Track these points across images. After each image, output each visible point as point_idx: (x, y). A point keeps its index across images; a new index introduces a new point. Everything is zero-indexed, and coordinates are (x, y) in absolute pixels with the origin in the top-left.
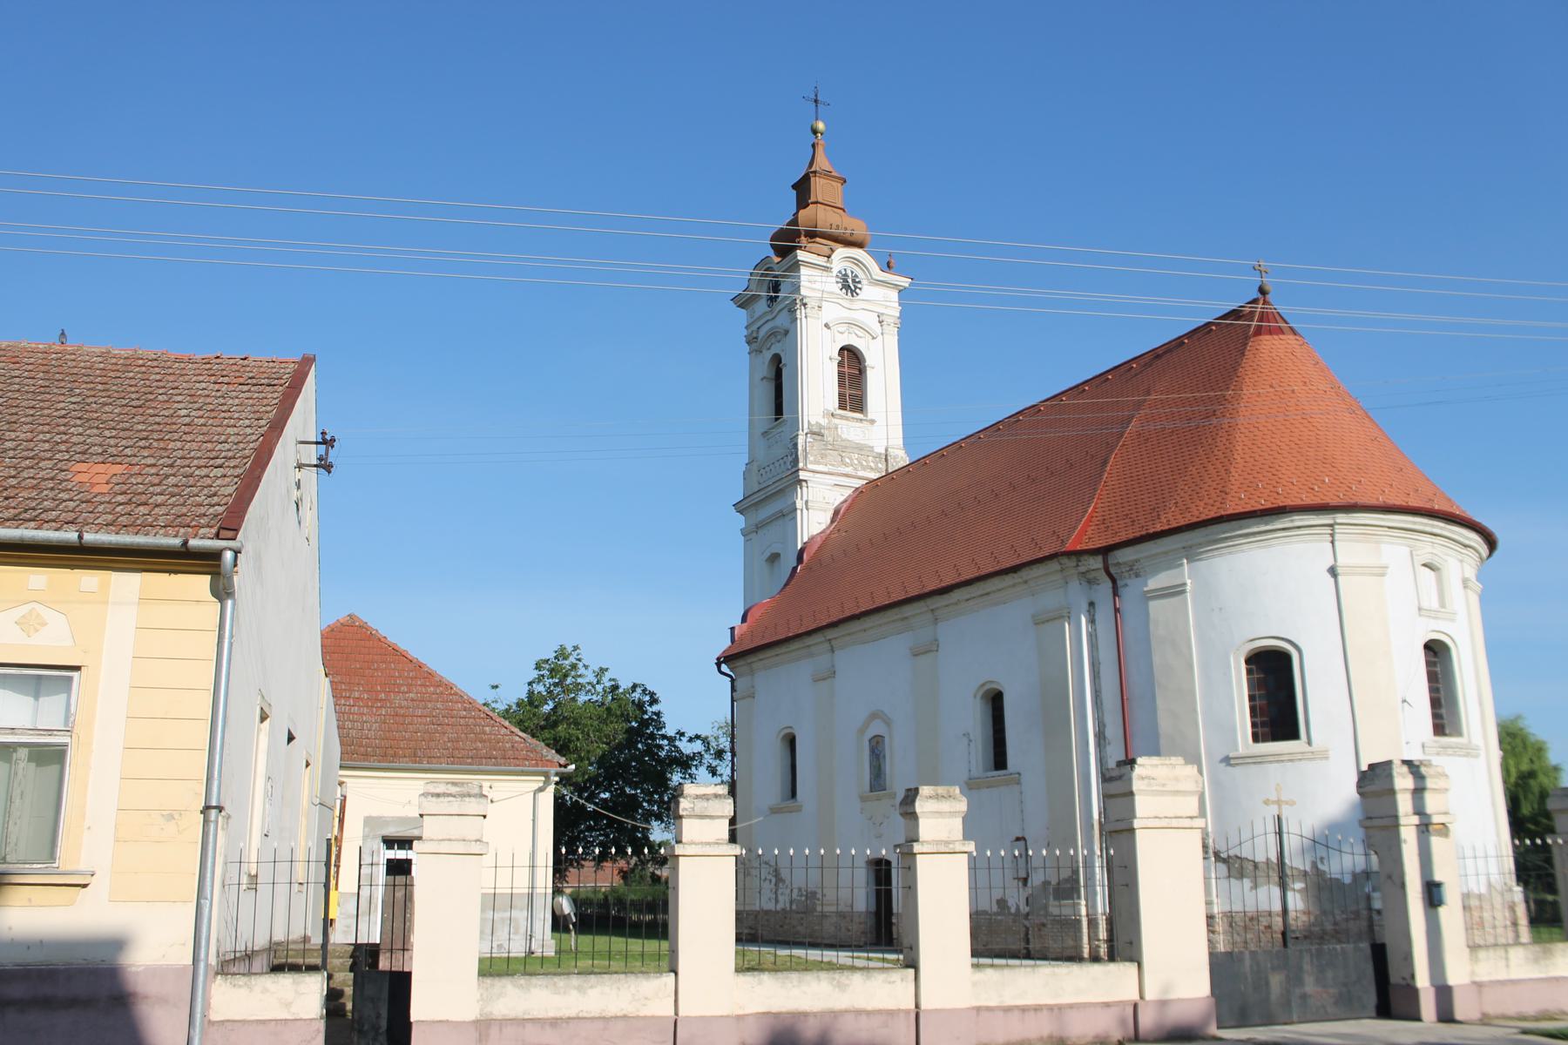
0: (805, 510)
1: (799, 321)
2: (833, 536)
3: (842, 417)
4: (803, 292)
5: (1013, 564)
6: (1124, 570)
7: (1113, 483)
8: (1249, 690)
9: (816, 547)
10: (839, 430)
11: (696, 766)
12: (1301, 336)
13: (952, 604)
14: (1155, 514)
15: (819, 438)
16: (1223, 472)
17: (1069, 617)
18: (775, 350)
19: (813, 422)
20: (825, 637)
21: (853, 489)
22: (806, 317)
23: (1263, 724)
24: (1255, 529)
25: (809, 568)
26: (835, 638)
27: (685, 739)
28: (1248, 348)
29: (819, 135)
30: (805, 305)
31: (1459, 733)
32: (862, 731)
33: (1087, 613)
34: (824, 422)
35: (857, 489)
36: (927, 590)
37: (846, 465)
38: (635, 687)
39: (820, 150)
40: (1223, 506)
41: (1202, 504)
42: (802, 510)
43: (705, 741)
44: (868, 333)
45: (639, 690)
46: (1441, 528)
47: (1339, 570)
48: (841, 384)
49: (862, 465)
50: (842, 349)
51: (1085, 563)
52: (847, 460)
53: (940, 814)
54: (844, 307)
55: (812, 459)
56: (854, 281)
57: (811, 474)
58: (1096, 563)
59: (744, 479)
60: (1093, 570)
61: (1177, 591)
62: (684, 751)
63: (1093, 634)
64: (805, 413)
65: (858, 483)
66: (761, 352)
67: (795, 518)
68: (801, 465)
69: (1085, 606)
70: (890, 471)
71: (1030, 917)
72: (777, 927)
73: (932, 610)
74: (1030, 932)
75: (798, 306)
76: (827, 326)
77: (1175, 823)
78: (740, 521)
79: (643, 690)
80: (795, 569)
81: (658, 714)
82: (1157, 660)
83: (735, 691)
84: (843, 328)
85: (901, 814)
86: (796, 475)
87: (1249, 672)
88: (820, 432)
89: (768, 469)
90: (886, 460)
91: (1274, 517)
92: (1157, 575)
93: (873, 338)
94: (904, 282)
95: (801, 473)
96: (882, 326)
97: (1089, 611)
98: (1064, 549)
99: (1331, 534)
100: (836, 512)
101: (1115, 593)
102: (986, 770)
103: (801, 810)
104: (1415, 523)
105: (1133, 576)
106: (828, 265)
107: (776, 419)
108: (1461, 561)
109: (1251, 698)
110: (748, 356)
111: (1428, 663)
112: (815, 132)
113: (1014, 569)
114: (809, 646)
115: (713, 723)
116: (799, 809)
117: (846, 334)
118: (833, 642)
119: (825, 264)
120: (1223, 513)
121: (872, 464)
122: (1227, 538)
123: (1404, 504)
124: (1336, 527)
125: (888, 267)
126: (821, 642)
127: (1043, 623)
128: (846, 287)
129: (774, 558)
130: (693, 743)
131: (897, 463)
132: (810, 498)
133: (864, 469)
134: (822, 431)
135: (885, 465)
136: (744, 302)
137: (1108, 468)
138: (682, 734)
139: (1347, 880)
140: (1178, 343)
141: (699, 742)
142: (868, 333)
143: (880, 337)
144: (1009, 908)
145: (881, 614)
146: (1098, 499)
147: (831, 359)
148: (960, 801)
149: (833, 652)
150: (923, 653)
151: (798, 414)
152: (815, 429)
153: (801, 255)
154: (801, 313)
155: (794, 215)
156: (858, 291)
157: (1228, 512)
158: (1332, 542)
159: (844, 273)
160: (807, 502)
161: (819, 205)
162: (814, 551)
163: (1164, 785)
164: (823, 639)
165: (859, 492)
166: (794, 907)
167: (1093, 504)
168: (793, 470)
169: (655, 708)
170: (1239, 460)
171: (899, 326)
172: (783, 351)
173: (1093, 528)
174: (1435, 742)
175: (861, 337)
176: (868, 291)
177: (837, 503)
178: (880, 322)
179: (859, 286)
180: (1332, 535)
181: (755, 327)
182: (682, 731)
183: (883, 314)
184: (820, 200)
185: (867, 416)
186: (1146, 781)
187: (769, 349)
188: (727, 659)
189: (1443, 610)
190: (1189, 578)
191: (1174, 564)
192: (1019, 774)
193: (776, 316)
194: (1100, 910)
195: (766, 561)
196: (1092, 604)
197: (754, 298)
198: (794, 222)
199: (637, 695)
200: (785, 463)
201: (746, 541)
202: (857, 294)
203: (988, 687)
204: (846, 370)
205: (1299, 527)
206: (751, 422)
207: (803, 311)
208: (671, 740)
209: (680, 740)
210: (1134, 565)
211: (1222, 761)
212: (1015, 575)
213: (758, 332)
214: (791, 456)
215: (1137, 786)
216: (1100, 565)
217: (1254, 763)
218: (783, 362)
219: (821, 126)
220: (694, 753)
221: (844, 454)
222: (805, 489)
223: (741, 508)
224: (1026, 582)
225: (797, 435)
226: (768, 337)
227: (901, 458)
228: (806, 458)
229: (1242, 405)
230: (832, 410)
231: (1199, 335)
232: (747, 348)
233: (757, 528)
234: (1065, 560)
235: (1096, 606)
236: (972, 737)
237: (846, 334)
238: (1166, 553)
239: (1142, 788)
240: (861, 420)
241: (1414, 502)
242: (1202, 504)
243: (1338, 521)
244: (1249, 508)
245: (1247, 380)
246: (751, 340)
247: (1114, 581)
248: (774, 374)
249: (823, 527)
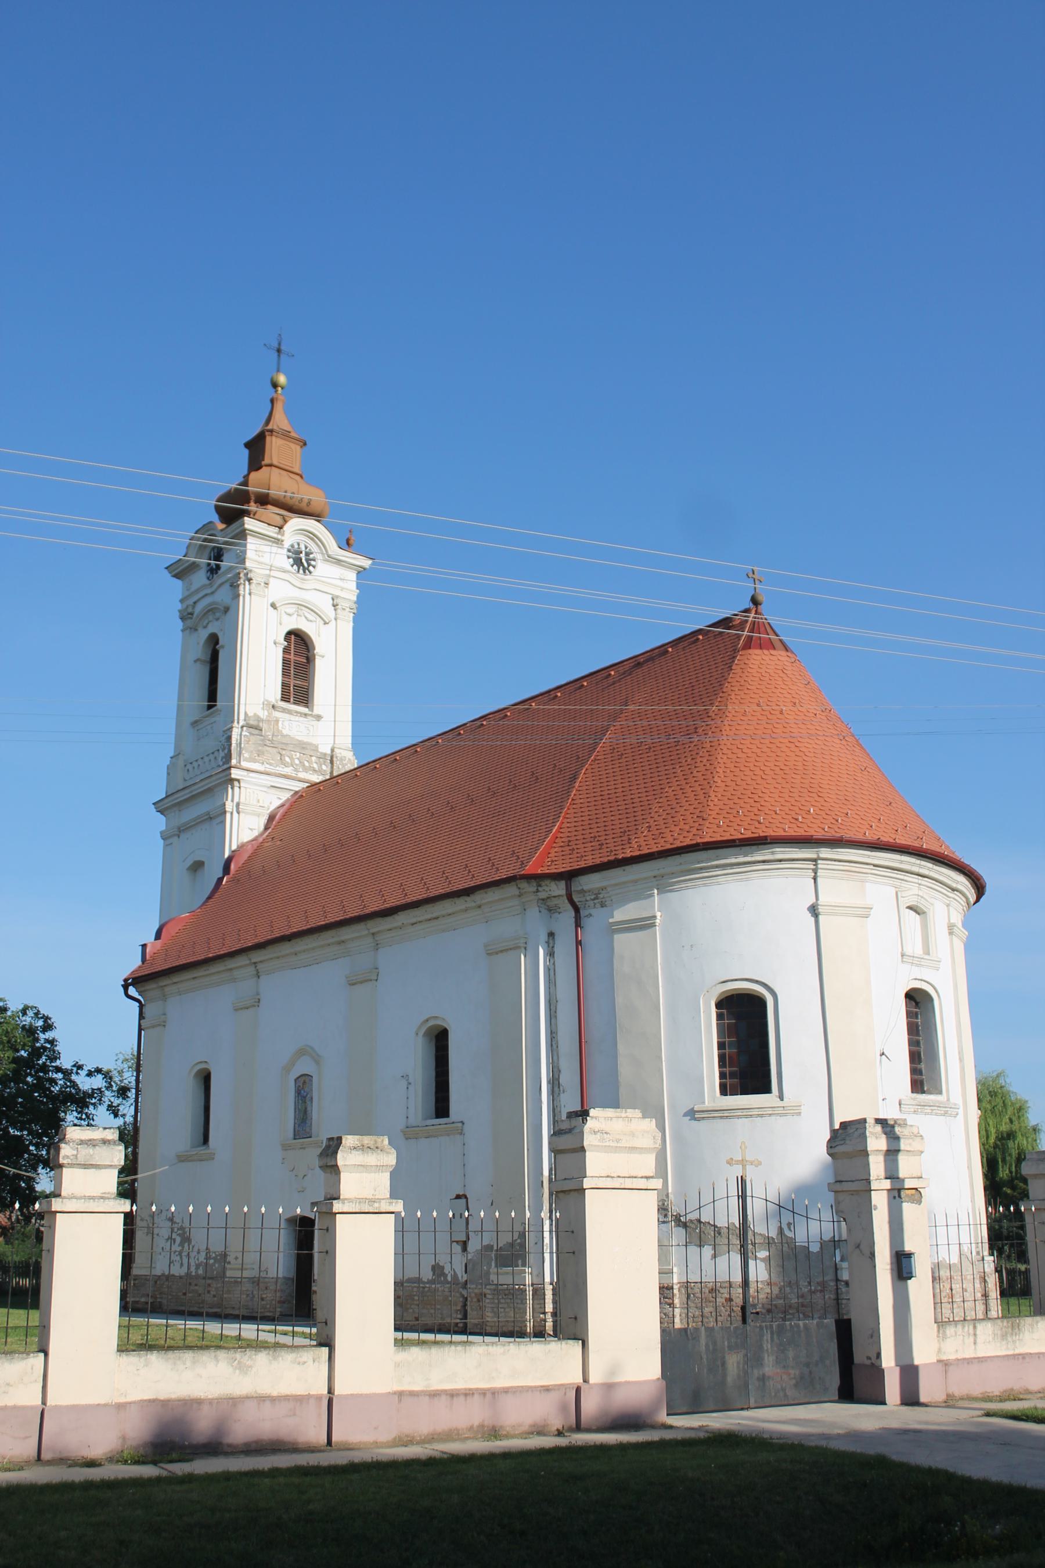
0: (235, 814)
1: (241, 598)
2: (266, 845)
3: (284, 710)
4: (248, 564)
5: (466, 886)
6: (588, 898)
7: (581, 801)
8: (718, 1037)
9: (245, 856)
10: (280, 723)
11: (94, 1104)
12: (792, 652)
13: (395, 928)
14: (625, 838)
15: (257, 732)
16: (702, 797)
17: (525, 948)
18: (212, 628)
19: (250, 714)
20: (250, 960)
21: (292, 793)
22: (250, 594)
23: (732, 1075)
24: (733, 860)
25: (235, 880)
26: (261, 962)
27: (83, 1073)
28: (736, 662)
29: (280, 389)
30: (249, 580)
31: (940, 1093)
32: (287, 1069)
33: (546, 945)
34: (263, 714)
35: (296, 792)
36: (367, 911)
37: (286, 765)
38: (24, 1012)
39: (279, 407)
40: (700, 832)
41: (677, 829)
42: (232, 813)
43: (107, 1076)
44: (320, 616)
45: (30, 1013)
46: (929, 869)
47: (821, 909)
48: (285, 672)
49: (304, 765)
50: (290, 633)
51: (545, 888)
52: (287, 759)
53: (364, 1168)
54: (294, 586)
55: (246, 755)
56: (307, 560)
57: (245, 773)
58: (558, 889)
59: (168, 774)
60: (554, 897)
61: (646, 924)
62: (81, 1086)
63: (552, 967)
64: (242, 701)
65: (298, 786)
66: (196, 630)
67: (223, 822)
68: (234, 762)
69: (543, 937)
70: (335, 774)
71: (468, 1286)
72: (180, 1294)
73: (373, 934)
74: (468, 1303)
75: (242, 581)
76: (273, 606)
77: (629, 1183)
78: (160, 822)
79: (35, 1014)
80: (220, 880)
81: (52, 1042)
82: (619, 1000)
83: (144, 1018)
84: (291, 609)
85: (320, 1167)
86: (227, 772)
87: (719, 1017)
88: (258, 726)
89: (195, 764)
90: (332, 762)
91: (754, 847)
92: (624, 905)
93: (325, 623)
94: (367, 563)
95: (233, 771)
96: (335, 610)
97: (548, 943)
98: (522, 873)
99: (813, 870)
100: (271, 818)
101: (578, 924)
102: (426, 1118)
103: (213, 1159)
104: (901, 862)
105: (598, 905)
106: (279, 537)
107: (210, 707)
108: (948, 905)
109: (721, 1046)
110: (181, 633)
111: (909, 1014)
112: (275, 385)
113: (467, 892)
114: (231, 969)
115: (117, 1055)
116: (211, 1157)
117: (295, 616)
118: (259, 966)
119: (275, 536)
120: (699, 841)
121: (315, 766)
122: (701, 868)
123: (892, 841)
124: (819, 862)
125: (347, 544)
126: (246, 965)
127: (497, 953)
128: (298, 562)
129: (197, 867)
130: (93, 1078)
131: (344, 766)
132: (242, 800)
133: (306, 770)
134: (261, 724)
135: (329, 767)
136: (181, 571)
137: (577, 784)
138: (80, 1067)
139: (815, 1248)
140: (661, 651)
141: (100, 1076)
142: (320, 616)
143: (334, 621)
144: (445, 1276)
145: (315, 936)
146: (565, 818)
147: (275, 643)
148: (388, 1153)
149: (259, 977)
150: (361, 982)
151: (234, 702)
152: (252, 722)
153: (249, 523)
154: (244, 588)
155: (244, 477)
156: (311, 568)
157: (705, 840)
158: (815, 879)
159: (296, 546)
160: (238, 805)
161: (273, 468)
162: (243, 862)
163: (618, 1141)
164: (248, 962)
165: (298, 797)
166: (201, 1272)
167: (558, 824)
168: (226, 766)
169: (49, 1035)
170: (720, 783)
171: (355, 611)
172: (221, 630)
173: (556, 850)
174: (914, 1099)
175: (311, 621)
176: (322, 569)
177: (272, 808)
178: (334, 606)
179: (313, 563)
180: (815, 871)
181: (191, 601)
182: (80, 1063)
183: (337, 597)
184: (275, 462)
185: (312, 711)
186: (598, 1136)
187: (205, 627)
188: (136, 981)
189: (926, 957)
190: (658, 911)
191: (643, 895)
192: (463, 1123)
193: (216, 590)
194: (547, 1279)
195: (188, 869)
196: (551, 935)
197: (193, 567)
198: (245, 483)
199: (27, 1020)
200: (215, 758)
201: (166, 846)
202: (310, 572)
203: (431, 1023)
204: (292, 657)
205: (780, 861)
206: (180, 708)
208: (67, 1073)
209: (77, 1073)
210: (600, 894)
211: (685, 1115)
212: (467, 899)
213: (194, 607)
214: (223, 750)
215: (588, 1140)
216: (563, 892)
217: (721, 1117)
218: (221, 642)
219: (282, 379)
220: (93, 1090)
221: (284, 752)
222: (236, 789)
223: (161, 807)
224: (479, 907)
225: (232, 727)
226: (205, 614)
227: (348, 761)
228: (240, 754)
229: (726, 723)
230: (273, 701)
231: (686, 643)
232: (180, 625)
233: (180, 832)
234: (523, 884)
235: (555, 937)
236: (411, 1080)
237: (295, 616)
238: (635, 881)
239: (596, 1143)
240: (306, 715)
241: (902, 840)
242: (677, 829)
243: (822, 856)
244: (727, 837)
245: (733, 697)
246: (186, 616)
247: (577, 910)
248: (209, 656)
249: (256, 833)
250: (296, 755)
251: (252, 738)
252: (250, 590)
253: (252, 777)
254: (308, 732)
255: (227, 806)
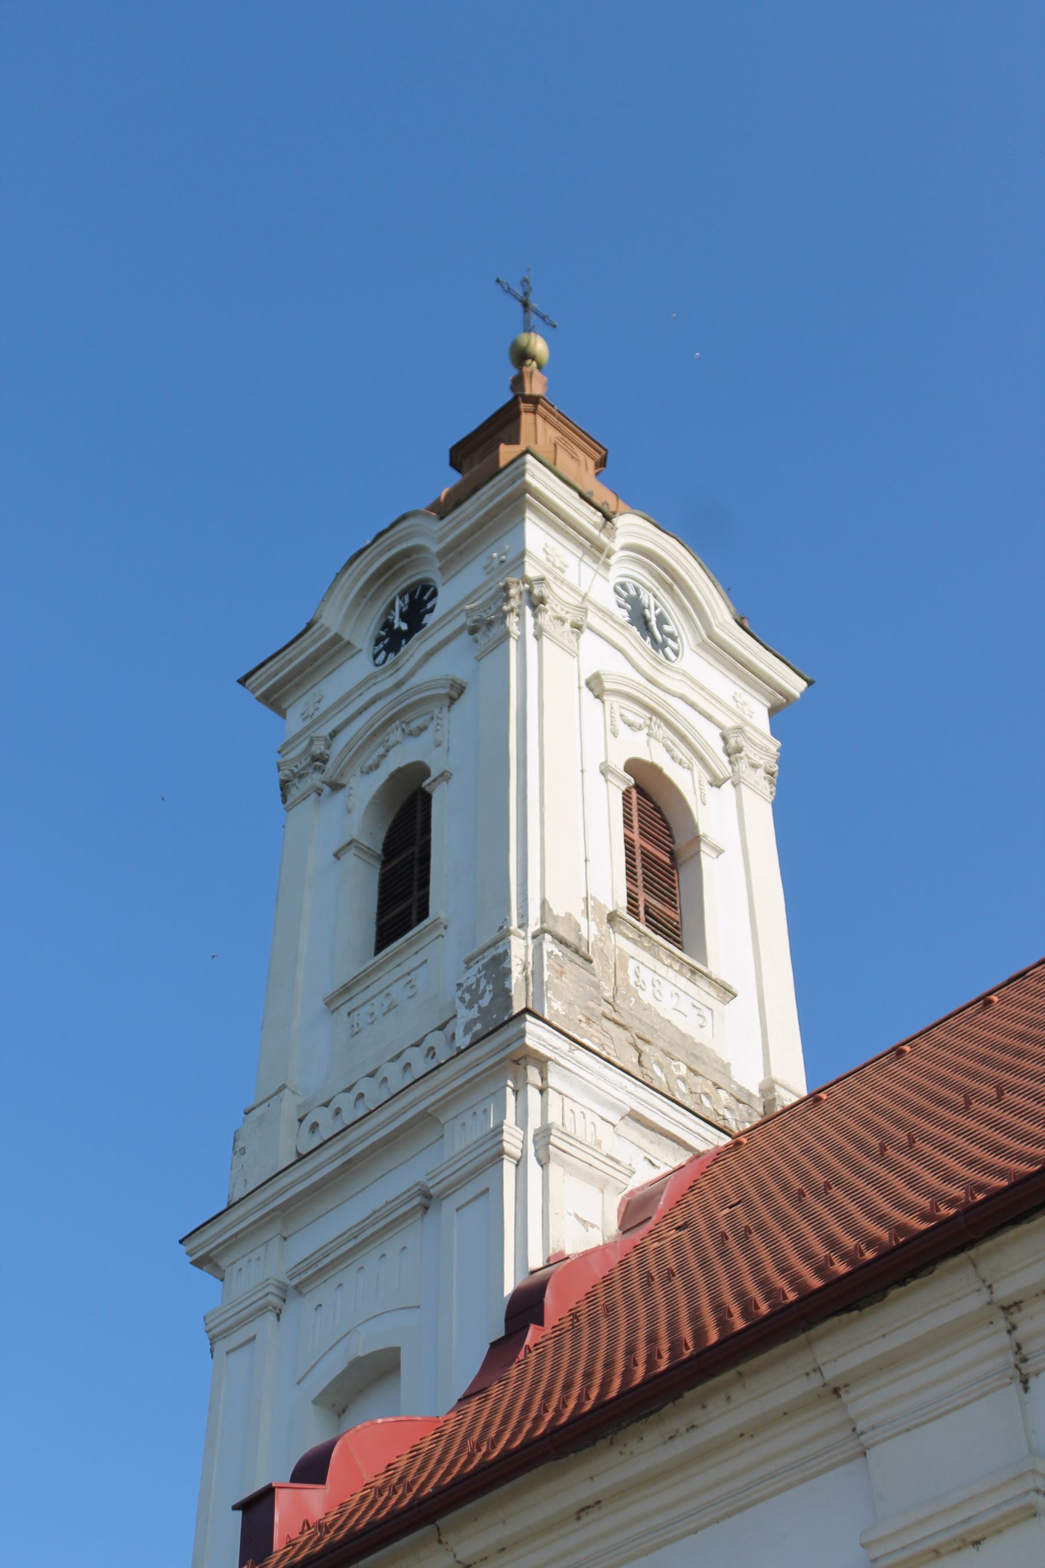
4: (531, 571)
19: (558, 909)
34: (591, 930)
57: (563, 1044)
67: (492, 1194)
76: (595, 685)
94: (796, 685)
95: (531, 1025)
112: (521, 356)
132: (554, 1117)
154: (522, 624)
160: (544, 1134)
207: (529, 620)
221: (646, 1048)
222: (533, 1095)
250: (678, 1068)
251: (569, 967)
252: (536, 624)
253: (579, 1064)
254: (700, 1021)
255: (505, 1136)
